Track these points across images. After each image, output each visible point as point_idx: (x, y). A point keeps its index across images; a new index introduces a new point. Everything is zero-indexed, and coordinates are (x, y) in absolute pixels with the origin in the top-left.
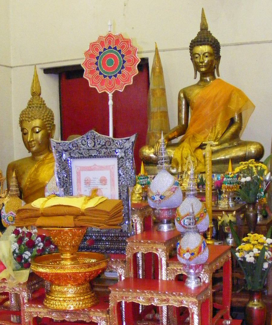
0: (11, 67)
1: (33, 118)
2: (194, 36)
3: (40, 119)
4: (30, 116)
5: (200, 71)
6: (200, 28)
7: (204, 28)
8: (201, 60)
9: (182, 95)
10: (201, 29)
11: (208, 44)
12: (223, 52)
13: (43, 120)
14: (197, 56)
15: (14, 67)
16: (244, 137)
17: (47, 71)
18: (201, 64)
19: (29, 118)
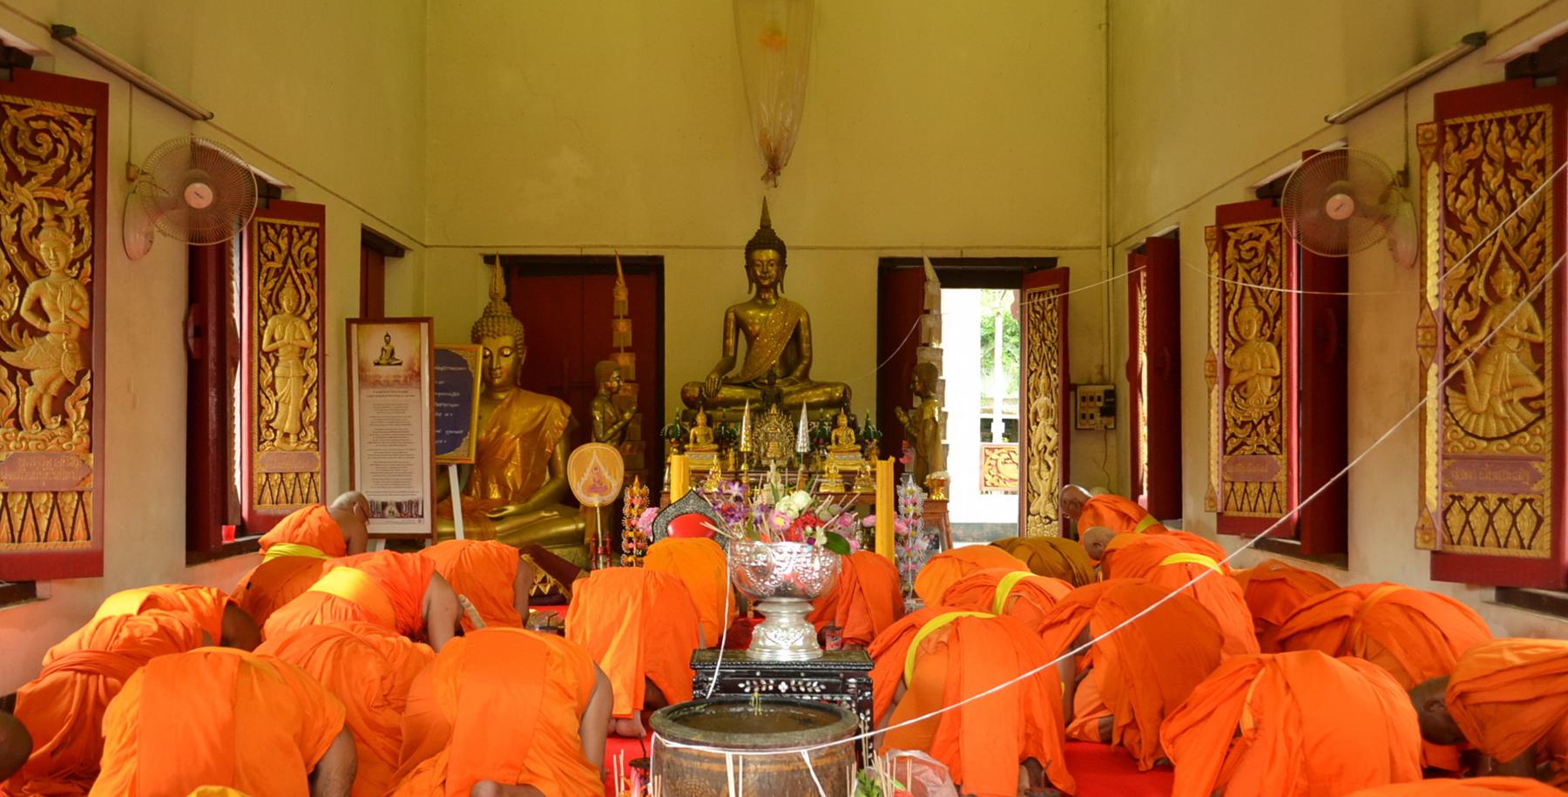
0: (426, 247)
2: (751, 235)
3: (511, 335)
6: (759, 224)
7: (765, 227)
9: (732, 316)
10: (762, 226)
15: (431, 246)
16: (814, 375)
17: (489, 260)
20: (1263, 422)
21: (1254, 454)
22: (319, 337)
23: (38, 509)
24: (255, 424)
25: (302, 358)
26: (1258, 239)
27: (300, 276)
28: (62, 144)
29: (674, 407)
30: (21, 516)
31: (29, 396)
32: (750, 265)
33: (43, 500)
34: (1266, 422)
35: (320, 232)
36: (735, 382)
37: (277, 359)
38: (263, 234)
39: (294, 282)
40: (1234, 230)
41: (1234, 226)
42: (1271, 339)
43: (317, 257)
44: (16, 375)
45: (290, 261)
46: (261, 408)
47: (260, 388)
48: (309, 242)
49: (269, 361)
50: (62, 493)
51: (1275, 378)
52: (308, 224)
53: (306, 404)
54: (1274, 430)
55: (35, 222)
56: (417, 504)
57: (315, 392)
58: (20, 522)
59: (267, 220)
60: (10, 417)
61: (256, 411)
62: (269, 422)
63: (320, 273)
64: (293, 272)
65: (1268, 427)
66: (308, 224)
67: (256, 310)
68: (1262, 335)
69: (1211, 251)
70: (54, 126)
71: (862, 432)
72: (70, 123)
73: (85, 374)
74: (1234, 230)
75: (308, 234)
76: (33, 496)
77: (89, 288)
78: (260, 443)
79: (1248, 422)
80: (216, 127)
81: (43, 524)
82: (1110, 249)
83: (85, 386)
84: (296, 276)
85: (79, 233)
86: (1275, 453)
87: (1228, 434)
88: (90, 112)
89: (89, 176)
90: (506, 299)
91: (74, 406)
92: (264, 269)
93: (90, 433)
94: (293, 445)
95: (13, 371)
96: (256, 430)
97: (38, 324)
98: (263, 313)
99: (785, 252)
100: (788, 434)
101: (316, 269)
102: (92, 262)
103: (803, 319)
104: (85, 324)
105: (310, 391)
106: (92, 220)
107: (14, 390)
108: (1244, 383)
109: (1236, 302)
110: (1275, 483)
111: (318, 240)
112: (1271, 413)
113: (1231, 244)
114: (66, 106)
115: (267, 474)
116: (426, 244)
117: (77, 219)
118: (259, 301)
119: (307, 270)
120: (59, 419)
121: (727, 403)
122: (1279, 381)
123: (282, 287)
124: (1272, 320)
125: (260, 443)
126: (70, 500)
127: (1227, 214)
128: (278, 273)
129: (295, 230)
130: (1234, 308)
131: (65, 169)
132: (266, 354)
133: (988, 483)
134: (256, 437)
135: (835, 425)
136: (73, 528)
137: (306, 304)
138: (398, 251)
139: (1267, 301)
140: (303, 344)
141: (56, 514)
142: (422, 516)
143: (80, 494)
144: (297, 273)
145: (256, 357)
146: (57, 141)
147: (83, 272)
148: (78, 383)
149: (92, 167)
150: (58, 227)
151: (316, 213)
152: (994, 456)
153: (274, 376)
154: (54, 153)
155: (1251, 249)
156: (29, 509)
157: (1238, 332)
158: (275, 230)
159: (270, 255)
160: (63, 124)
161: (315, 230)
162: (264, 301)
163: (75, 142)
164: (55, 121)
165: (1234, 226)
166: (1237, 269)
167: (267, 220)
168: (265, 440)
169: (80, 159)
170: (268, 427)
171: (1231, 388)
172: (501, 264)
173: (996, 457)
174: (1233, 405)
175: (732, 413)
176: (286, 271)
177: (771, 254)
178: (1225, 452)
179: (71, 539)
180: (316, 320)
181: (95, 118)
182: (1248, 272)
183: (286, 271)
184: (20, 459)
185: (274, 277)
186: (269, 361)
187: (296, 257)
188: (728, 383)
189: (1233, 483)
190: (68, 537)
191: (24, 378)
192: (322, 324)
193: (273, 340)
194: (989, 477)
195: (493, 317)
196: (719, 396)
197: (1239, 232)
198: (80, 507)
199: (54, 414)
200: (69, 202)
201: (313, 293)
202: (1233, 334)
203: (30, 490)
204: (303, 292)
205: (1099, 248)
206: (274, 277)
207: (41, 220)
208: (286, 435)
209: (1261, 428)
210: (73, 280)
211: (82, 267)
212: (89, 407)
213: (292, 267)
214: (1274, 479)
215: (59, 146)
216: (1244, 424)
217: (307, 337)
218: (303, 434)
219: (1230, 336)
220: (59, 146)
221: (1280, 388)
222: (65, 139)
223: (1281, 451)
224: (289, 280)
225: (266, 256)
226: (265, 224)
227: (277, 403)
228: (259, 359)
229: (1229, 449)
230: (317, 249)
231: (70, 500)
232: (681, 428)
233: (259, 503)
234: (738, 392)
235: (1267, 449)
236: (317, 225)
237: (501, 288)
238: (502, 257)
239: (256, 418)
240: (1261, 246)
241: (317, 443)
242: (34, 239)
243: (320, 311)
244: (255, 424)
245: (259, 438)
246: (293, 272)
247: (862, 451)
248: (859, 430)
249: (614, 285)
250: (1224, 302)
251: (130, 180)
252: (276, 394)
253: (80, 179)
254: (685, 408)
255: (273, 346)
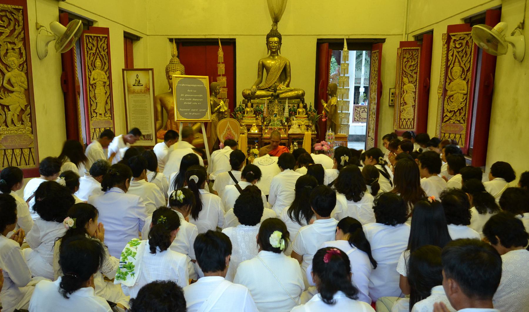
0: (148, 35)
1: (174, 71)
2: (268, 32)
4: (174, 69)
5: (271, 50)
8: (274, 45)
9: (261, 63)
11: (277, 37)
12: (283, 41)
13: (181, 71)
14: (271, 42)
17: (171, 40)
18: (273, 47)
19: (174, 70)
20: (459, 112)
21: (454, 123)
22: (110, 78)
23: (16, 154)
24: (90, 111)
25: (104, 86)
26: (463, 39)
27: (102, 55)
28: (12, 20)
29: (240, 99)
30: (11, 157)
31: (9, 115)
32: (268, 43)
33: (18, 152)
34: (460, 111)
35: (108, 38)
36: (262, 88)
37: (95, 86)
38: (88, 41)
39: (100, 58)
40: (454, 35)
41: (454, 34)
42: (465, 79)
43: (107, 48)
44: (4, 108)
45: (98, 50)
46: (91, 105)
47: (90, 98)
48: (104, 42)
49: (93, 88)
50: (24, 148)
51: (465, 94)
52: (103, 35)
53: (107, 103)
54: (463, 114)
55: (5, 51)
56: (150, 135)
57: (109, 98)
58: (11, 159)
59: (89, 34)
60: (4, 123)
61: (89, 106)
62: (94, 110)
63: (108, 53)
64: (99, 54)
65: (460, 113)
66: (103, 35)
67: (87, 69)
68: (461, 78)
69: (444, 44)
70: (8, 14)
71: (308, 110)
72: (14, 12)
73: (28, 106)
74: (454, 35)
75: (104, 39)
76: (14, 150)
77: (27, 74)
78: (91, 118)
79: (453, 111)
80: (67, 3)
81: (18, 160)
82: (406, 35)
83: (28, 110)
84: (100, 56)
85: (21, 54)
86: (462, 123)
87: (444, 115)
88: (21, 7)
89: (23, 32)
90: (178, 57)
91: (25, 118)
92: (89, 53)
93: (32, 127)
94: (103, 118)
95: (3, 106)
96: (90, 113)
97: (10, 88)
98: (90, 70)
99: (281, 38)
100: (281, 111)
101: (107, 52)
102: (27, 65)
103: (288, 64)
104: (26, 87)
105: (108, 98)
106: (25, 49)
107: (4, 113)
108: (452, 96)
109: (452, 64)
110: (461, 134)
111: (107, 41)
112: (462, 108)
113: (452, 41)
114: (12, 6)
115: (95, 129)
116: (148, 34)
117: (20, 49)
118: (88, 66)
119: (104, 53)
120: (21, 123)
121: (259, 97)
122: (466, 96)
123: (96, 59)
124: (466, 72)
125: (91, 118)
126: (26, 152)
127: (451, 29)
128: (94, 54)
129: (99, 38)
130: (451, 66)
131: (14, 30)
132: (92, 85)
133: (356, 120)
134: (90, 116)
135: (298, 107)
136: (29, 161)
137: (104, 66)
138: (138, 38)
139: (465, 64)
140: (104, 80)
141: (22, 156)
142: (152, 140)
143: (30, 149)
144: (101, 54)
145: (88, 87)
146: (10, 19)
147: (24, 68)
148: (26, 110)
149: (23, 29)
150: (13, 52)
151: (106, 31)
152: (359, 110)
153: (95, 93)
154: (9, 24)
155: (460, 43)
156: (13, 155)
157: (452, 76)
158: (92, 38)
159: (90, 48)
160: (11, 13)
161: (106, 37)
162: (90, 66)
163: (16, 19)
164: (8, 12)
165: (454, 34)
166: (454, 51)
167: (89, 34)
168: (93, 117)
169: (19, 26)
170: (94, 112)
171: (447, 97)
172: (176, 42)
173: (360, 110)
174: (447, 103)
175: (261, 101)
176: (97, 53)
177: (276, 39)
178: (442, 121)
179: (29, 165)
180: (108, 72)
181: (23, 9)
182: (458, 52)
183: (97, 53)
184: (8, 138)
185: (93, 56)
186: (93, 88)
187: (100, 49)
188: (260, 89)
189: (445, 133)
190: (28, 164)
191: (7, 109)
192: (110, 73)
193: (94, 79)
194: (356, 117)
195: (173, 64)
196: (256, 94)
197: (456, 36)
198: (30, 153)
199: (19, 121)
200: (16, 41)
201: (106, 62)
202: (450, 76)
203: (13, 148)
204: (103, 62)
205: (402, 35)
206: (93, 56)
207: (7, 50)
208: (101, 114)
209: (458, 114)
210: (21, 72)
211: (23, 67)
212: (31, 118)
213: (99, 52)
214: (461, 133)
215: (11, 21)
216: (451, 112)
217: (106, 78)
218: (106, 114)
219: (448, 77)
220: (11, 21)
221: (466, 99)
222: (12, 18)
223: (464, 122)
224: (98, 56)
225: (89, 48)
226: (88, 36)
227: (96, 103)
228: (89, 87)
229: (445, 121)
230: (107, 45)
231: (26, 152)
232: (242, 108)
233: (93, 139)
234: (263, 93)
235: (459, 121)
236: (106, 36)
237: (176, 53)
238: (175, 39)
239: (90, 109)
240: (464, 42)
241: (111, 117)
242: (5, 57)
243: (109, 68)
244: (90, 111)
245: (91, 116)
246: (99, 54)
247: (308, 117)
248: (307, 109)
249: (218, 50)
250: (447, 64)
251: (38, 29)
252: (96, 99)
253: (20, 34)
254: (244, 99)
255: (94, 82)
